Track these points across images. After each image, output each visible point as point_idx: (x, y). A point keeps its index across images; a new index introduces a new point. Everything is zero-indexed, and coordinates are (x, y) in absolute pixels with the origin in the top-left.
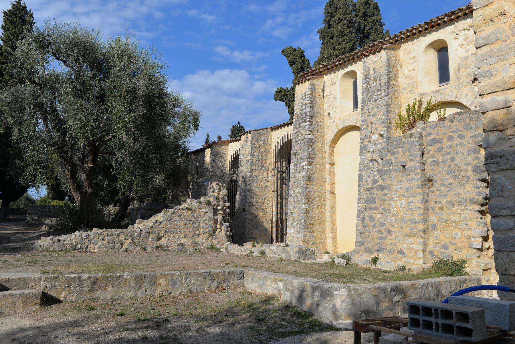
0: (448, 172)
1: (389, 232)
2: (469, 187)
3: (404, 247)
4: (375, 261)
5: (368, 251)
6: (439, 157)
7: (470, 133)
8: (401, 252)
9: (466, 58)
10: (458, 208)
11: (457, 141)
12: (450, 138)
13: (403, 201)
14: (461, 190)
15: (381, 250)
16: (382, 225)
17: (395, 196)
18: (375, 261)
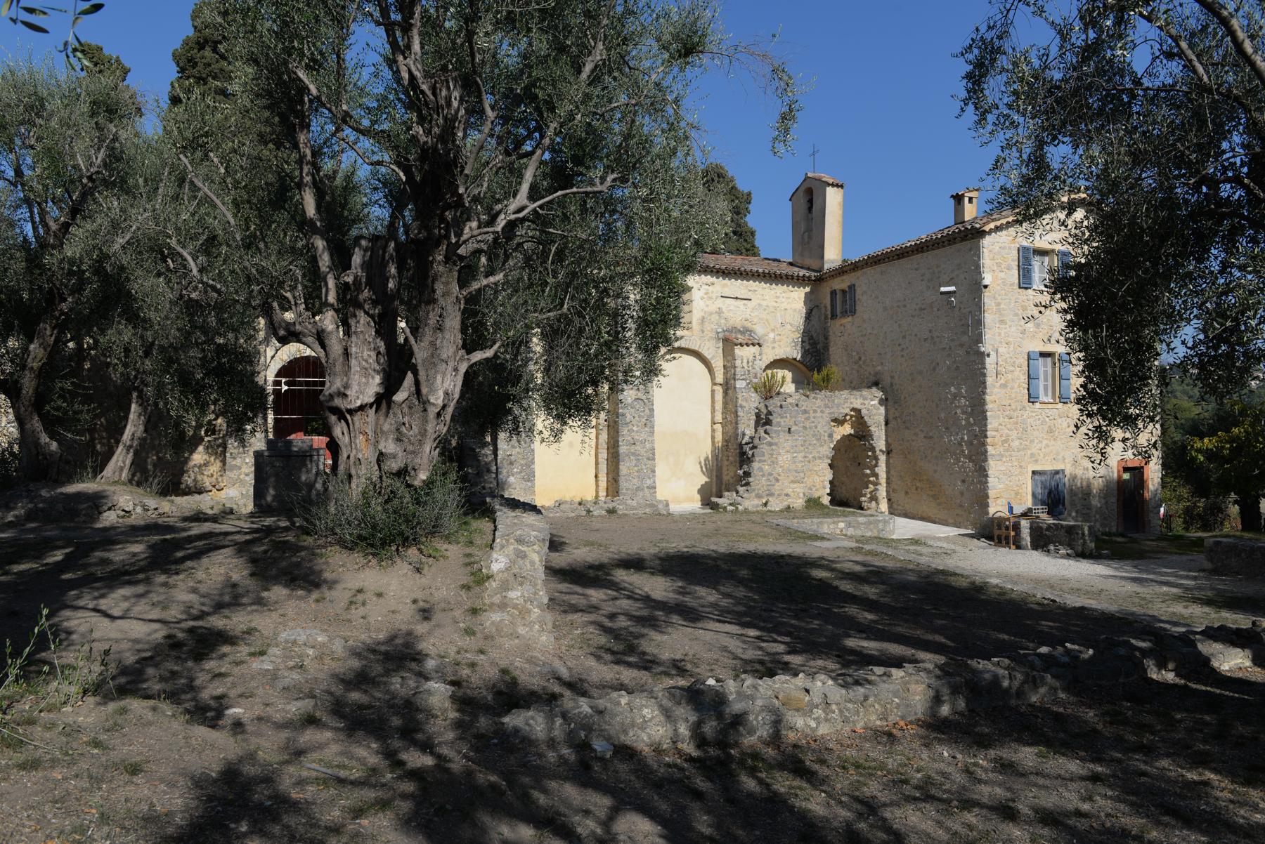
0: (814, 436)
1: (777, 480)
2: (826, 447)
3: (789, 491)
4: (766, 504)
5: (759, 496)
6: (807, 424)
7: (827, 411)
8: (787, 495)
9: (711, 314)
10: (818, 461)
11: (818, 414)
12: (815, 411)
13: (789, 455)
14: (821, 449)
15: (772, 495)
16: (770, 474)
17: (782, 452)
18: (766, 504)
